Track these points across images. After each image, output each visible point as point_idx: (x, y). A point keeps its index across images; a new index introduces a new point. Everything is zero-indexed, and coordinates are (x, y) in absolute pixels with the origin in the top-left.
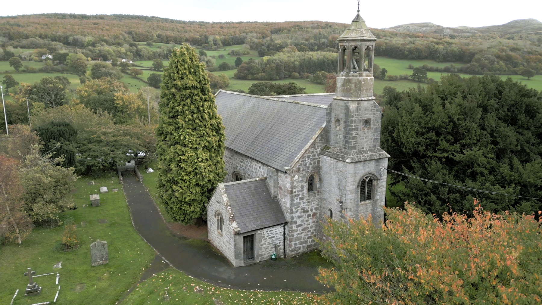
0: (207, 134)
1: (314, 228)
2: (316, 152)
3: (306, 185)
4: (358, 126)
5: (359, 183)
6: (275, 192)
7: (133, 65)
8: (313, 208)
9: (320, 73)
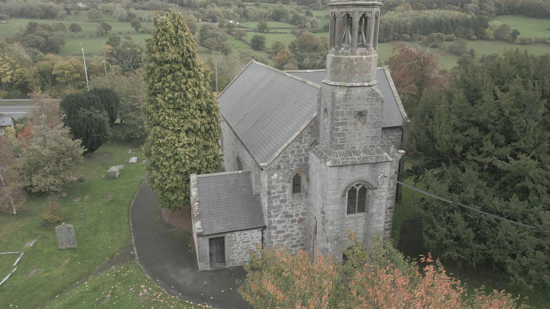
0: (192, 115)
1: (300, 236)
2: (303, 147)
3: (289, 186)
4: (346, 119)
5: (345, 192)
6: (256, 189)
7: (240, 27)
8: (299, 213)
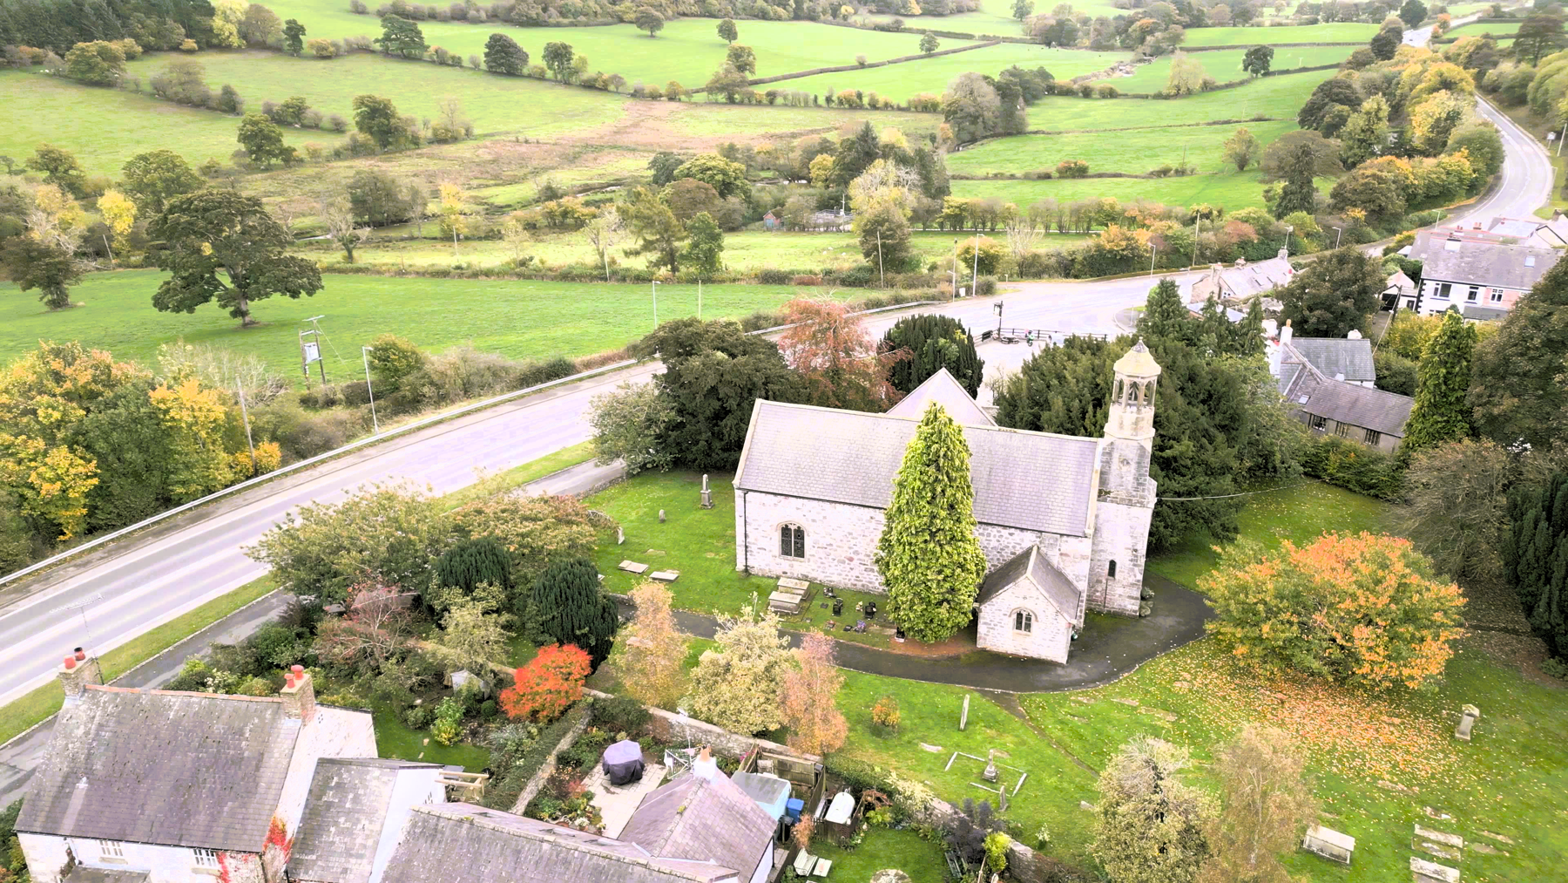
9: (92, 47)
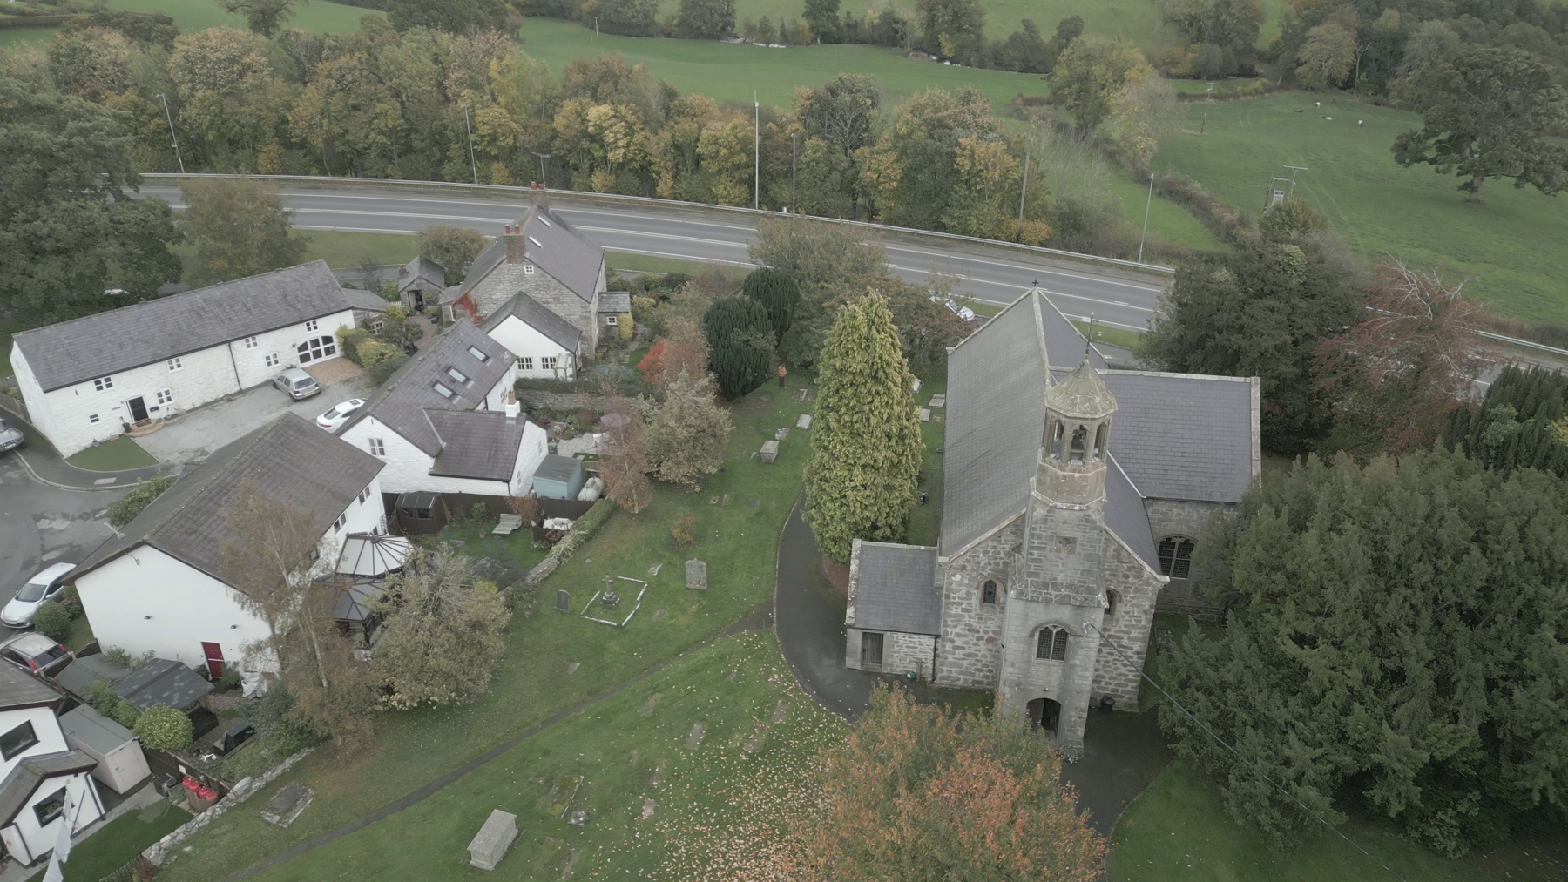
3: (977, 595)
